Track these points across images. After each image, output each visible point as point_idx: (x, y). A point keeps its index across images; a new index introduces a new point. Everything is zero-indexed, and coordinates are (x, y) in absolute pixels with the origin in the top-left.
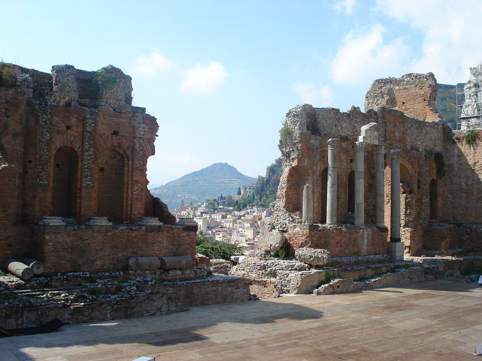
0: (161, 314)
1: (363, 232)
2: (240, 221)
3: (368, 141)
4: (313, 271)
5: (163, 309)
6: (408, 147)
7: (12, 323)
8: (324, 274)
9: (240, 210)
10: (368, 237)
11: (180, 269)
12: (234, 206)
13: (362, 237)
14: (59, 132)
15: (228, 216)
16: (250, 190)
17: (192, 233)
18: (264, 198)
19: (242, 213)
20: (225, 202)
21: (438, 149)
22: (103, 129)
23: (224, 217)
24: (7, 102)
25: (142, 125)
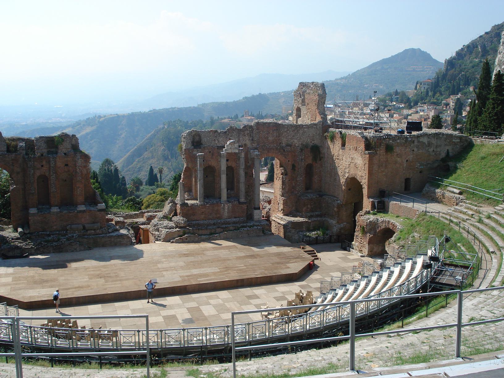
0: (77, 251)
3: (230, 151)
4: (177, 229)
5: (78, 249)
6: (284, 145)
7: (11, 254)
8: (182, 231)
9: (410, 107)
10: (228, 209)
11: (94, 230)
12: (405, 103)
13: (224, 208)
15: (395, 115)
16: (425, 86)
17: (103, 212)
18: (438, 94)
19: (410, 112)
20: (398, 98)
21: (317, 142)
22: (60, 164)
24: (13, 160)
25: (80, 160)
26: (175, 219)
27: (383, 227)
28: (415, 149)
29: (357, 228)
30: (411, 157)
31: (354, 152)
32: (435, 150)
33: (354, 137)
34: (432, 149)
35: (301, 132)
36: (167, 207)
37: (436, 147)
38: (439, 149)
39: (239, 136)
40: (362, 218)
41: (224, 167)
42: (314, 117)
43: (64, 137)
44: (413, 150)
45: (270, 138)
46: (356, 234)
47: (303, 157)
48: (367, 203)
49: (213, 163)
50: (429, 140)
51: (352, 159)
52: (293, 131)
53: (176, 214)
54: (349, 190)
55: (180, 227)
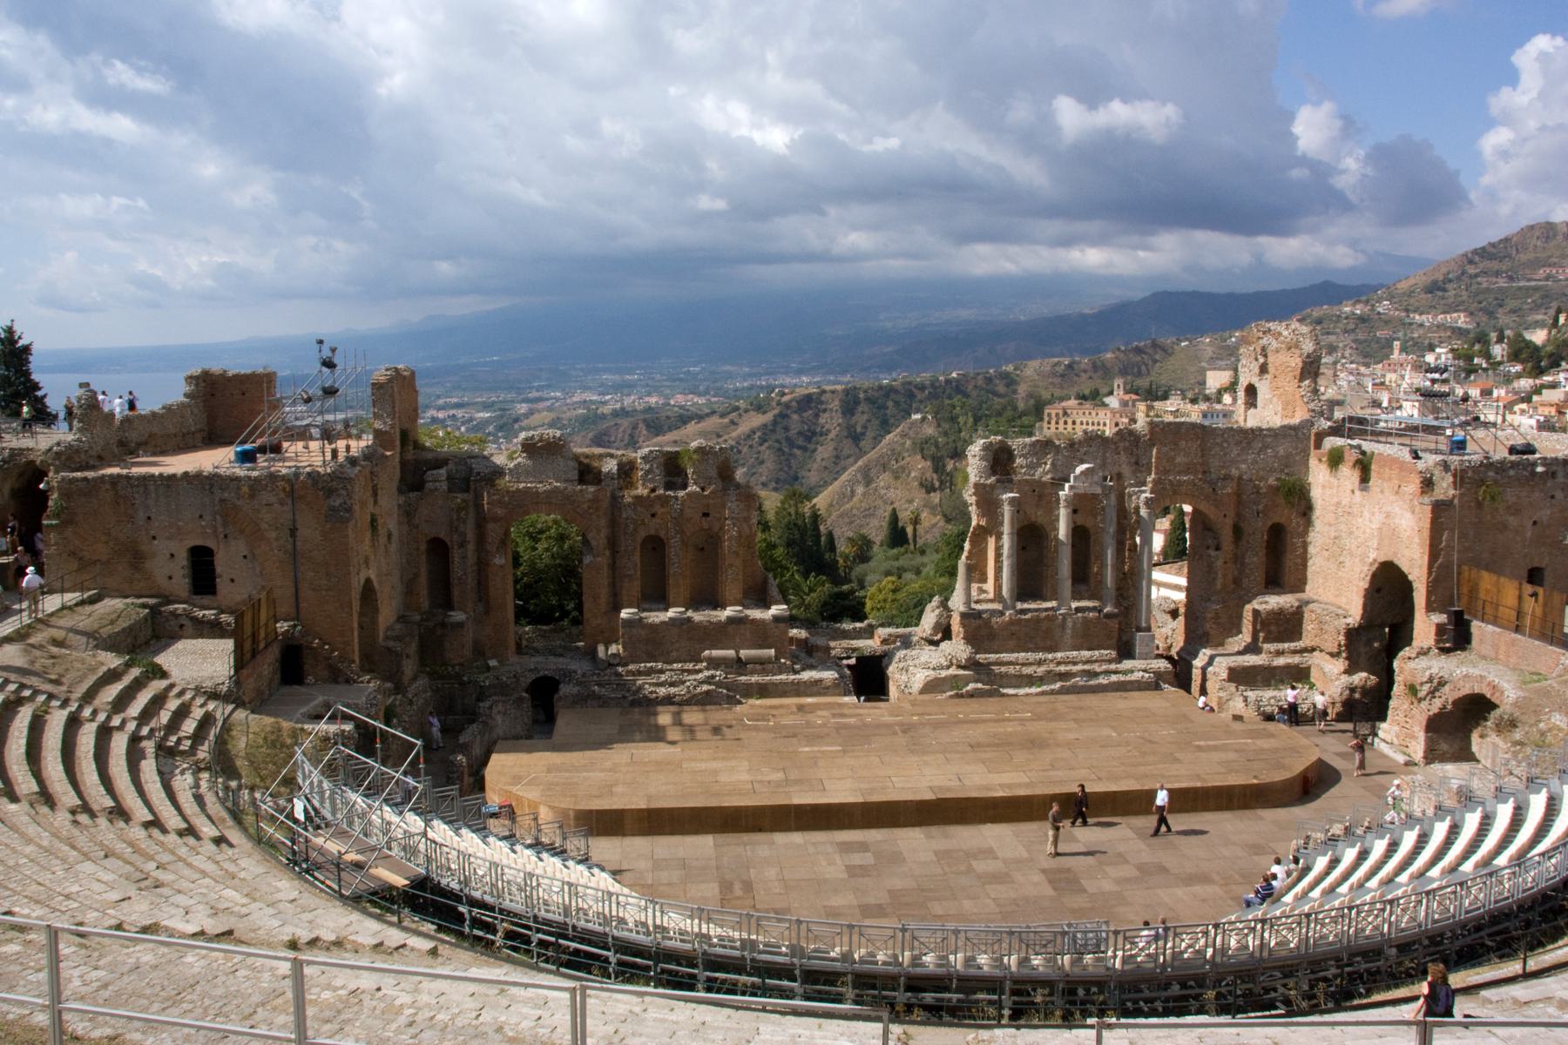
1: (1064, 619)
2: (1524, 406)
13: (1063, 626)
23: (1486, 393)
26: (944, 645)
27: (1466, 690)
28: (1559, 495)
29: (1398, 689)
30: (1544, 514)
31: (1393, 498)
33: (1393, 461)
36: (929, 618)
40: (1412, 665)
41: (1063, 531)
42: (1288, 406)
45: (1178, 460)
46: (1392, 703)
47: (1261, 507)
48: (1425, 626)
49: (1039, 516)
51: (1387, 517)
52: (1238, 443)
53: (947, 634)
54: (1378, 590)
55: (959, 667)
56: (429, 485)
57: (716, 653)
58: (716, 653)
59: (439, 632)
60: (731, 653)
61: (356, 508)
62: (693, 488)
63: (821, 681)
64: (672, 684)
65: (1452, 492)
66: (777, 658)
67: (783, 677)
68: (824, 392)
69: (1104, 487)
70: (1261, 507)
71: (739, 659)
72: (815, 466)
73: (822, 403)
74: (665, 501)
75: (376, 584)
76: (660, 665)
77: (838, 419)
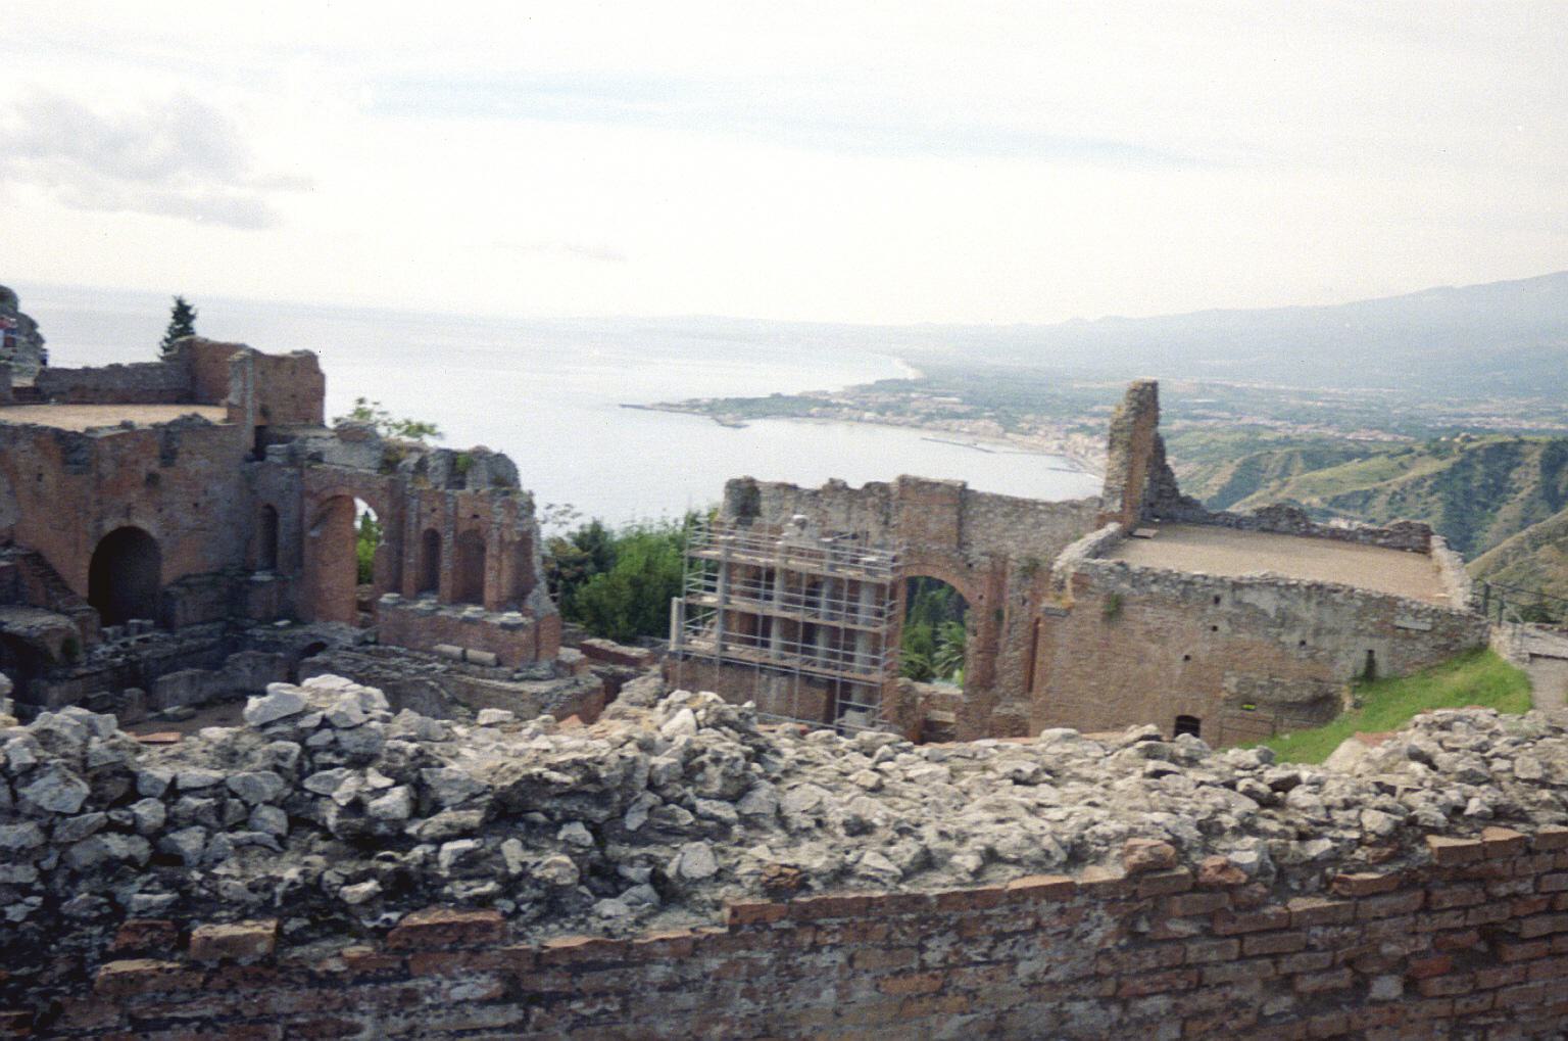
10: (778, 689)
14: (426, 515)
28: (1224, 627)
30: (1202, 649)
32: (1310, 642)
34: (1295, 638)
35: (1030, 520)
37: (1317, 633)
38: (1327, 643)
39: (850, 508)
43: (480, 454)
44: (1215, 629)
50: (1284, 603)
52: (1006, 515)
56: (269, 458)
57: (447, 648)
58: (447, 648)
59: (246, 587)
60: (457, 650)
61: (108, 467)
62: (469, 489)
63: (521, 692)
64: (398, 669)
65: (1073, 600)
66: (499, 663)
67: (496, 683)
68: (1522, 442)
69: (820, 544)
70: (1027, 594)
71: (464, 658)
72: (1495, 527)
73: (1516, 454)
74: (443, 497)
75: (154, 534)
76: (402, 650)
77: (1535, 475)
